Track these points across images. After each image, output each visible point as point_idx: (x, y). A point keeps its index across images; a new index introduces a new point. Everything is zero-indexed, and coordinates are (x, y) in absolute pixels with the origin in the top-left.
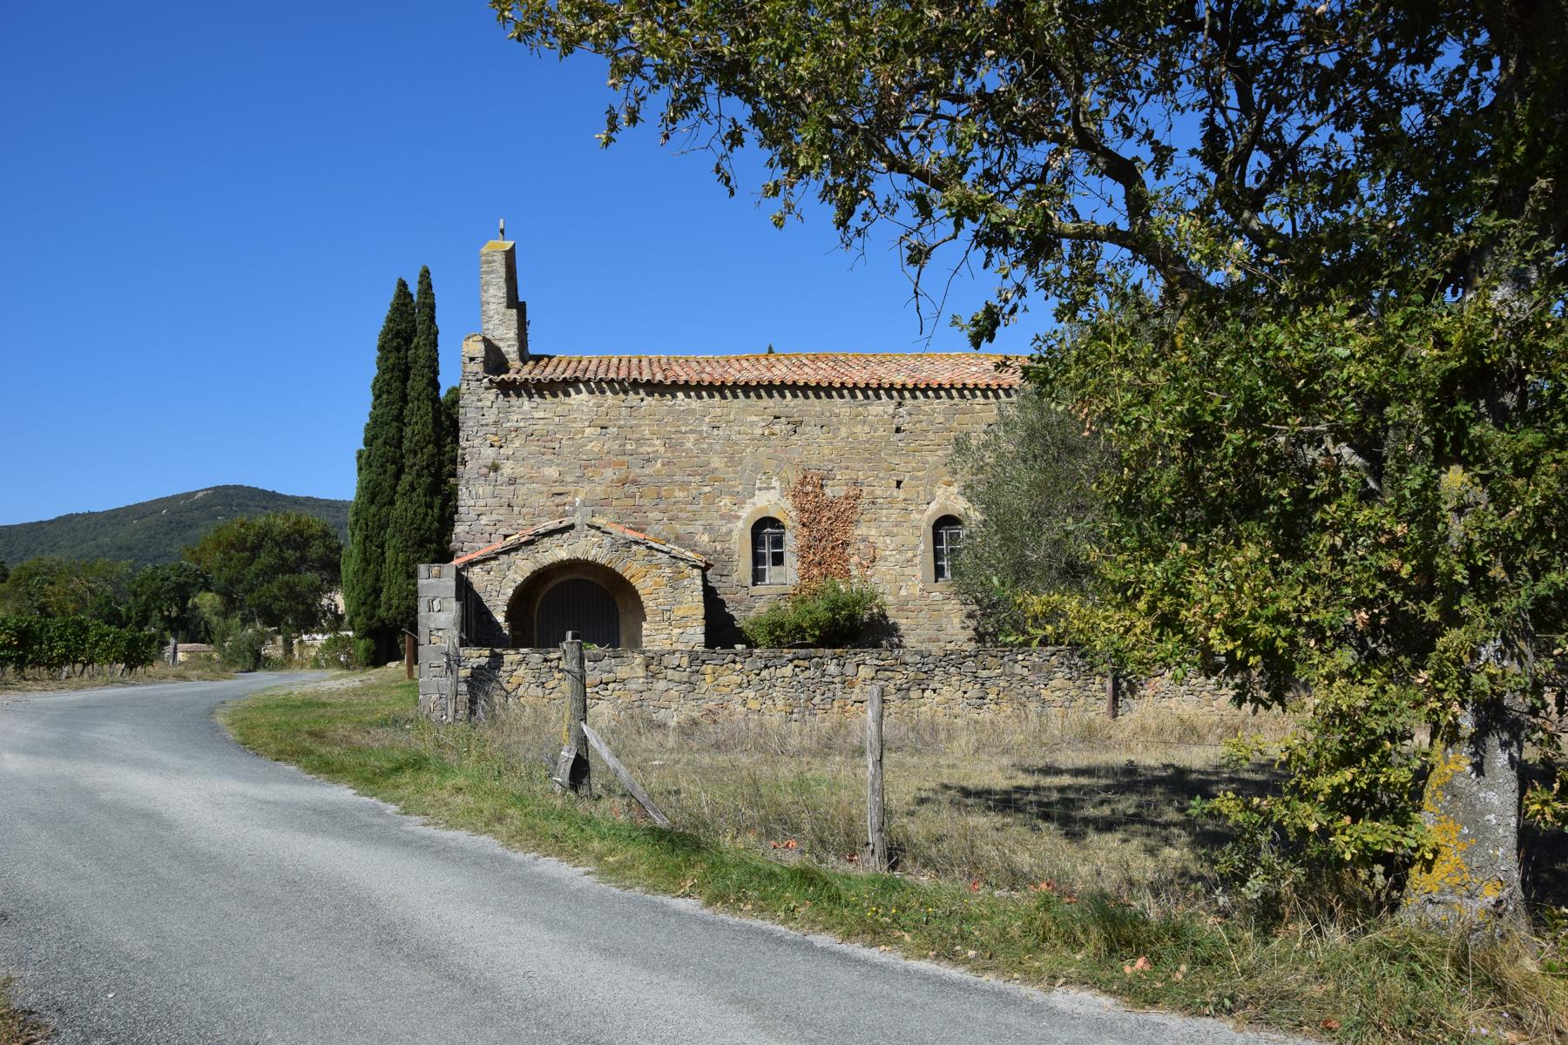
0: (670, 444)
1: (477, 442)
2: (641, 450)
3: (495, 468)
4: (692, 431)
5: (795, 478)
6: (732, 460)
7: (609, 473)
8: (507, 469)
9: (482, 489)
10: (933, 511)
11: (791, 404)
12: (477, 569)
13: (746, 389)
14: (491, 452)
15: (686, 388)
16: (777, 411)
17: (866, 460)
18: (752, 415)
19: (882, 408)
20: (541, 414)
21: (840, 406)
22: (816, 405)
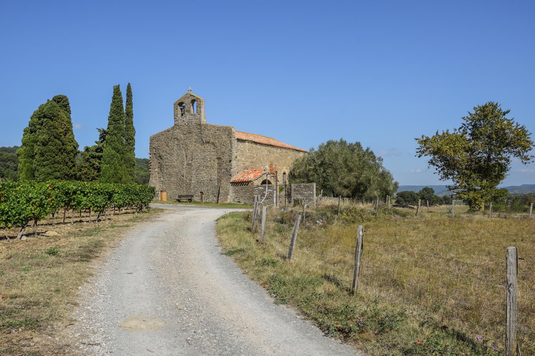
3: (236, 157)
5: (270, 163)
6: (263, 159)
7: (250, 160)
9: (235, 162)
10: (282, 172)
14: (236, 154)
15: (260, 144)
19: (279, 151)
21: (274, 150)
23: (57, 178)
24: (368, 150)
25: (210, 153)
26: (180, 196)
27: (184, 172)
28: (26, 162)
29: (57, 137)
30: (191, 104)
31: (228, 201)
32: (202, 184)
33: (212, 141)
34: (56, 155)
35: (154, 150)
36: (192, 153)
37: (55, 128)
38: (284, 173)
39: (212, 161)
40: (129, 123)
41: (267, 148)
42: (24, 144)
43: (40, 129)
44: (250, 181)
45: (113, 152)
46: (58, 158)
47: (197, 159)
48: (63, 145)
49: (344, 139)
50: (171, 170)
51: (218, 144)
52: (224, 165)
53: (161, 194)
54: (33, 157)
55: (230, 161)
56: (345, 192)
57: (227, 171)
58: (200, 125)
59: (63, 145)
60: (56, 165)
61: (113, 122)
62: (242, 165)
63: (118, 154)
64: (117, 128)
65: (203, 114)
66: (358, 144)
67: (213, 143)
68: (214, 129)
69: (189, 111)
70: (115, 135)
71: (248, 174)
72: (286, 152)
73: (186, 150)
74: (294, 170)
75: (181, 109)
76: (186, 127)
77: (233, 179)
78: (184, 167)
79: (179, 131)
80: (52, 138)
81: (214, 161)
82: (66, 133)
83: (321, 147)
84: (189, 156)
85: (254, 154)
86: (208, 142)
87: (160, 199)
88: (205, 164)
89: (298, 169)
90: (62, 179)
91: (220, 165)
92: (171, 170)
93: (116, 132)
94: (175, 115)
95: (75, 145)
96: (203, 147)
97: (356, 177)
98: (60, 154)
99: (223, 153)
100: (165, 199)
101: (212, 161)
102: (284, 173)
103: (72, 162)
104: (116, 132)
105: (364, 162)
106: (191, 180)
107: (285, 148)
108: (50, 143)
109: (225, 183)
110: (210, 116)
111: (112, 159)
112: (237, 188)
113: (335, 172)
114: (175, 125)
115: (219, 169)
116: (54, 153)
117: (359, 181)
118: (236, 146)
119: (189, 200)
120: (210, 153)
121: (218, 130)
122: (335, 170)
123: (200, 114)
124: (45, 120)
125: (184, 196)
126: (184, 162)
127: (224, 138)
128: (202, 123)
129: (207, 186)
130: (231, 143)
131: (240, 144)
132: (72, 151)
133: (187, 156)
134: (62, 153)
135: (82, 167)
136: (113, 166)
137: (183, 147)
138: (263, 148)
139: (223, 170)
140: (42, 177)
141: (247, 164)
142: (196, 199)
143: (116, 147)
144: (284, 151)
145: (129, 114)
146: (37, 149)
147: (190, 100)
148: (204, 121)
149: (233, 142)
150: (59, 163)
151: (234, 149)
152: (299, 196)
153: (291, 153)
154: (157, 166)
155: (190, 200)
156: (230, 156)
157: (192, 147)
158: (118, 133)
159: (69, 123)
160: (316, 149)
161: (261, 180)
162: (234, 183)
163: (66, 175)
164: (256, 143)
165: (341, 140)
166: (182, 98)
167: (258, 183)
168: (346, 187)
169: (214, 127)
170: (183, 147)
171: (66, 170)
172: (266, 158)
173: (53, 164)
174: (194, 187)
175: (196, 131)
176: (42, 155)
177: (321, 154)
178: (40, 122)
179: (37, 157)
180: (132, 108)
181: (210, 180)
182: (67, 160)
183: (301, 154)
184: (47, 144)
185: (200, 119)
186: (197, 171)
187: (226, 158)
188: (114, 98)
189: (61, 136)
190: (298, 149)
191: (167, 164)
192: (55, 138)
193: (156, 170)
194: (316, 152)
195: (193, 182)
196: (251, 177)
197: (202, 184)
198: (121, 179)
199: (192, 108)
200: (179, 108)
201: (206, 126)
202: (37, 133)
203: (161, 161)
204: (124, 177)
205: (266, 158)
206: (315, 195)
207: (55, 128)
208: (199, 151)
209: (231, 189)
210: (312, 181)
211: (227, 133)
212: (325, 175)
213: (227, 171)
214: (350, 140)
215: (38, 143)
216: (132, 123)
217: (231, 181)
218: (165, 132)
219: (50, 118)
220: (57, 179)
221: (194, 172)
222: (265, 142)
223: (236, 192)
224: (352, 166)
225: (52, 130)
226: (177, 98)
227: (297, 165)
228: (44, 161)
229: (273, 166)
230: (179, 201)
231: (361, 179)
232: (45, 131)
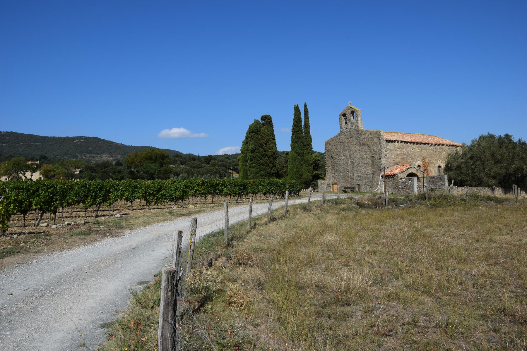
0: (408, 152)
3: (386, 155)
5: (422, 158)
6: (415, 156)
8: (388, 156)
9: (384, 159)
10: (438, 165)
13: (417, 143)
15: (409, 142)
18: (416, 148)
19: (432, 147)
21: (427, 147)
22: (425, 146)
23: (262, 176)
24: (520, 141)
25: (366, 153)
26: (346, 188)
27: (349, 169)
28: (243, 165)
33: (367, 143)
36: (354, 153)
37: (259, 140)
38: (439, 167)
40: (308, 132)
41: (419, 145)
42: (242, 152)
45: (295, 155)
46: (262, 161)
48: (265, 151)
49: (491, 133)
51: (371, 146)
54: (247, 161)
55: (380, 159)
56: (492, 182)
58: (358, 130)
59: (265, 151)
60: (261, 167)
65: (360, 121)
69: (349, 120)
70: (297, 142)
72: (440, 148)
79: (343, 136)
80: (257, 147)
83: (473, 141)
84: (352, 156)
85: (404, 152)
86: (364, 144)
93: (297, 140)
99: (375, 152)
100: (336, 191)
102: (439, 167)
103: (272, 164)
104: (297, 140)
107: (438, 145)
108: (256, 151)
110: (363, 123)
113: (483, 164)
115: (373, 165)
120: (366, 153)
127: (375, 140)
128: (360, 129)
129: (365, 179)
130: (380, 144)
131: (389, 144)
132: (272, 156)
134: (265, 158)
135: (283, 167)
138: (415, 145)
139: (376, 166)
141: (397, 160)
142: (356, 189)
144: (438, 147)
145: (307, 126)
146: (249, 155)
147: (351, 110)
148: (361, 127)
150: (262, 165)
156: (380, 154)
157: (353, 149)
158: (298, 141)
160: (469, 143)
161: (406, 173)
164: (406, 142)
166: (344, 110)
168: (494, 177)
169: (368, 131)
172: (417, 154)
174: (356, 180)
177: (471, 148)
182: (268, 162)
183: (459, 149)
185: (358, 126)
187: (377, 156)
188: (295, 115)
193: (330, 167)
196: (397, 171)
198: (302, 175)
199: (352, 117)
200: (343, 118)
201: (362, 131)
206: (447, 185)
207: (259, 140)
211: (377, 136)
212: (473, 167)
221: (355, 168)
222: (417, 141)
226: (341, 111)
228: (253, 164)
232: (253, 142)
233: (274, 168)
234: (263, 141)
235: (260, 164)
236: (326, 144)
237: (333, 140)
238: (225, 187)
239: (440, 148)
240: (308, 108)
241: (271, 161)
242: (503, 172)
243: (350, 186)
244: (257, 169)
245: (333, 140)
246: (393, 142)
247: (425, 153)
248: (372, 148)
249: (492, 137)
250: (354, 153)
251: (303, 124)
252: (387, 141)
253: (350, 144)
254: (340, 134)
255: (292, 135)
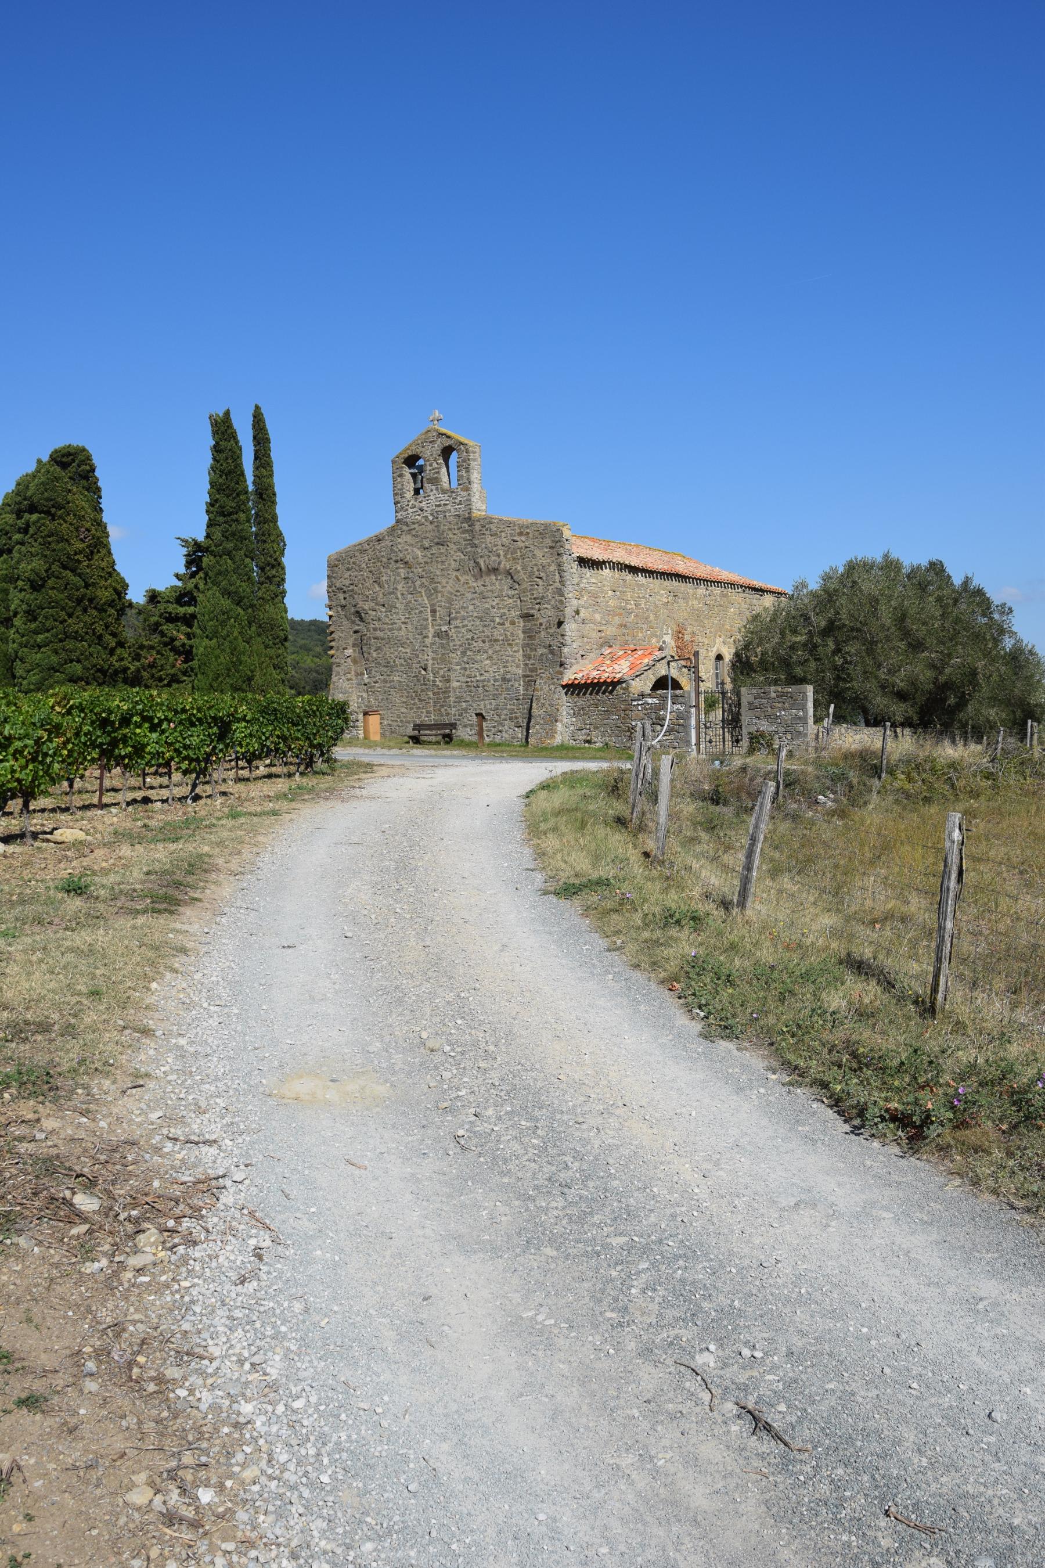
1: (570, 595)
2: (629, 606)
3: (577, 612)
4: (644, 597)
6: (657, 617)
7: (617, 620)
9: (574, 626)
11: (674, 584)
12: (637, 679)
14: (575, 602)
16: (669, 588)
17: (696, 621)
19: (701, 590)
20: (593, 580)
21: (688, 588)
23: (73, 680)
26: (418, 727)
29: (70, 565)
30: (441, 461)
31: (558, 740)
32: (480, 690)
33: (505, 565)
34: (70, 616)
35: (341, 596)
36: (450, 601)
37: (62, 540)
38: (719, 657)
39: (507, 624)
40: (268, 519)
41: (667, 583)
43: (22, 544)
44: (620, 682)
45: (226, 603)
46: (75, 625)
47: (464, 619)
48: (87, 586)
49: (894, 555)
50: (390, 653)
51: (522, 576)
52: (543, 635)
53: (365, 722)
55: (560, 624)
56: (899, 710)
57: (552, 652)
58: (469, 519)
59: (87, 586)
60: (70, 644)
61: (221, 519)
62: (595, 635)
63: (240, 610)
64: (233, 534)
65: (476, 487)
66: (936, 568)
67: (509, 573)
68: (509, 531)
69: (435, 481)
70: (229, 554)
71: (614, 659)
72: (723, 595)
73: (432, 593)
74: (746, 647)
75: (414, 476)
76: (430, 527)
77: (568, 677)
78: (428, 641)
79: (408, 538)
80: (55, 567)
81: (513, 623)
82: (92, 553)
83: (826, 578)
85: (627, 601)
86: (495, 570)
87: (361, 736)
88: (487, 633)
89: (760, 644)
90: (88, 683)
91: (530, 634)
92: (390, 653)
93: (230, 545)
94: (399, 494)
95: (119, 587)
96: (480, 583)
97: (933, 667)
98: (79, 612)
99: (539, 601)
100: (375, 736)
101: (507, 624)
102: (719, 657)
103: (114, 635)
104: (230, 545)
105: (957, 621)
106: (448, 681)
107: (718, 583)
108: (50, 582)
109: (546, 688)
111: (223, 624)
112: (581, 701)
113: (870, 652)
114: (398, 521)
116: (63, 609)
117: (942, 679)
118: (575, 581)
119: (444, 736)
120: (501, 601)
121: (521, 534)
122: (870, 648)
123: (467, 489)
124: (35, 517)
125: (429, 727)
126: (426, 628)
127: (542, 556)
128: (476, 514)
129: (495, 697)
130: (561, 571)
131: (588, 573)
132: (111, 604)
133: (434, 611)
134: (85, 610)
135: (142, 647)
136: (227, 644)
137: (422, 585)
138: (656, 583)
139: (541, 651)
140: (34, 679)
141: (610, 631)
142: (463, 733)
143: (232, 588)
144: (717, 591)
145: (265, 494)
148: (480, 507)
149: (566, 567)
150: (77, 637)
151: (570, 588)
152: (764, 722)
153: (736, 597)
154: (351, 641)
155: (448, 739)
156: (560, 608)
157: (447, 585)
159: (101, 526)
160: (814, 584)
161: (651, 679)
162: (573, 688)
163: (98, 670)
164: (634, 570)
165: (886, 556)
166: (415, 443)
167: (643, 685)
168: (901, 696)
169: (509, 524)
170: (422, 585)
171: (99, 657)
172: (663, 612)
173: (61, 641)
174: (459, 700)
175: (459, 537)
176: (31, 615)
177: (827, 597)
178: (20, 523)
179: (17, 622)
180: (271, 476)
181: (504, 679)
182: (99, 629)
183: (768, 601)
184: (43, 586)
185: (468, 503)
186: (464, 653)
187: (546, 615)
189: (79, 562)
190: (757, 584)
191: (379, 634)
192: (65, 567)
193: (349, 652)
194: (813, 595)
195: (455, 684)
196: (622, 669)
197: (480, 690)
198: (250, 679)
199: (444, 470)
200: (407, 472)
202: (15, 554)
203: (361, 627)
204: (258, 674)
205: (663, 612)
206: (811, 721)
207: (62, 540)
208: (469, 596)
209: (565, 703)
210: (803, 681)
211: (548, 541)
212: (839, 661)
213: (552, 652)
214: (913, 556)
215: (20, 583)
216: (274, 519)
217: (565, 682)
218: (369, 542)
219: (48, 513)
220: (75, 682)
221: (456, 657)
223: (578, 712)
224: (921, 635)
225: (53, 546)
227: (757, 630)
228: (36, 632)
229: (687, 638)
230: (416, 740)
231: (947, 671)
233: (119, 651)
234: (80, 546)
235: (67, 636)
236: (333, 566)
237: (363, 551)
238: (153, 728)
239: (723, 595)
240: (269, 426)
241: (107, 626)
242: (925, 676)
243: (432, 719)
244: (56, 652)
245: (363, 551)
246: (596, 564)
247: (682, 611)
248: (526, 585)
249: (891, 566)
250: (450, 601)
251: (251, 488)
252: (584, 562)
253: (433, 568)
254: (392, 529)
255: (210, 525)
